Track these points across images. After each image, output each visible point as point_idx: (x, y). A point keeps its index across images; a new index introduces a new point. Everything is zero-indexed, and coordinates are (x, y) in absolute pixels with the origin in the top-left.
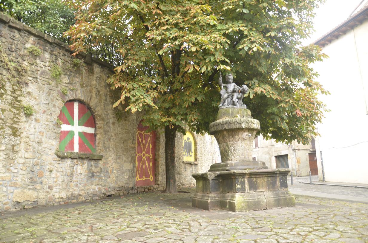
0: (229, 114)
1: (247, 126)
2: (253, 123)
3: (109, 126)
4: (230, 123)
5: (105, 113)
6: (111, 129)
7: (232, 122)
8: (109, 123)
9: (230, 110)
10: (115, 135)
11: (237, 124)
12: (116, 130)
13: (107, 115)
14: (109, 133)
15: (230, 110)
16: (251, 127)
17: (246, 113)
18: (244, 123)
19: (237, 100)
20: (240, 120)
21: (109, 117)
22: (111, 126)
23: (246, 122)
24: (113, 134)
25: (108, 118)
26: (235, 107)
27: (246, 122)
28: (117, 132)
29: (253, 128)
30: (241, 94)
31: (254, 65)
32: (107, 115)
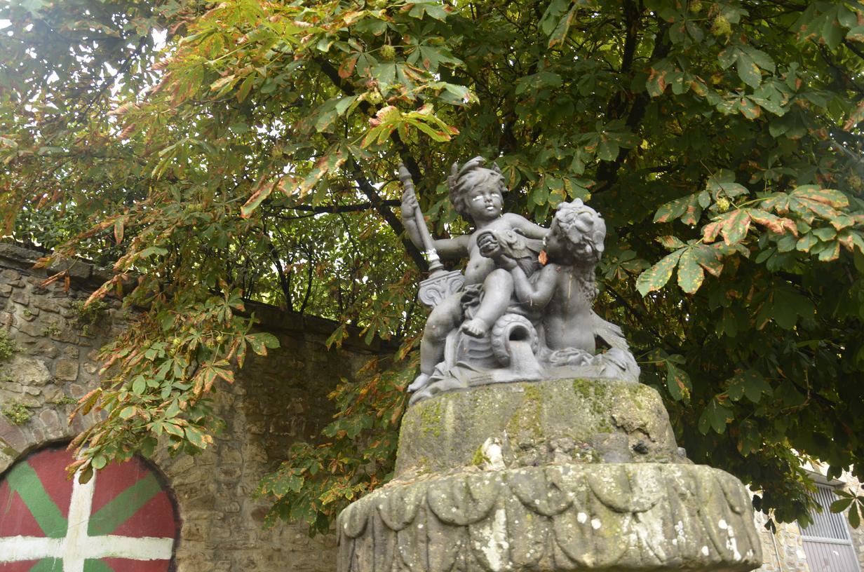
0: (441, 439)
1: (530, 555)
2: (618, 511)
3: (238, 528)
4: (386, 528)
5: (222, 477)
6: (247, 538)
7: (401, 511)
8: (239, 512)
9: (450, 408)
10: (270, 558)
11: (437, 534)
12: (275, 538)
13: (228, 484)
14: (238, 555)
15: (450, 408)
16: (588, 559)
17: (597, 410)
18: (501, 515)
19: (515, 320)
20: (468, 491)
21: (239, 490)
22: (251, 524)
23: (529, 506)
24: (255, 556)
25: (235, 495)
26: (499, 375)
27: (529, 506)
28: (277, 546)
29: (609, 558)
30: (550, 272)
31: (677, 90)
32: (231, 486)
